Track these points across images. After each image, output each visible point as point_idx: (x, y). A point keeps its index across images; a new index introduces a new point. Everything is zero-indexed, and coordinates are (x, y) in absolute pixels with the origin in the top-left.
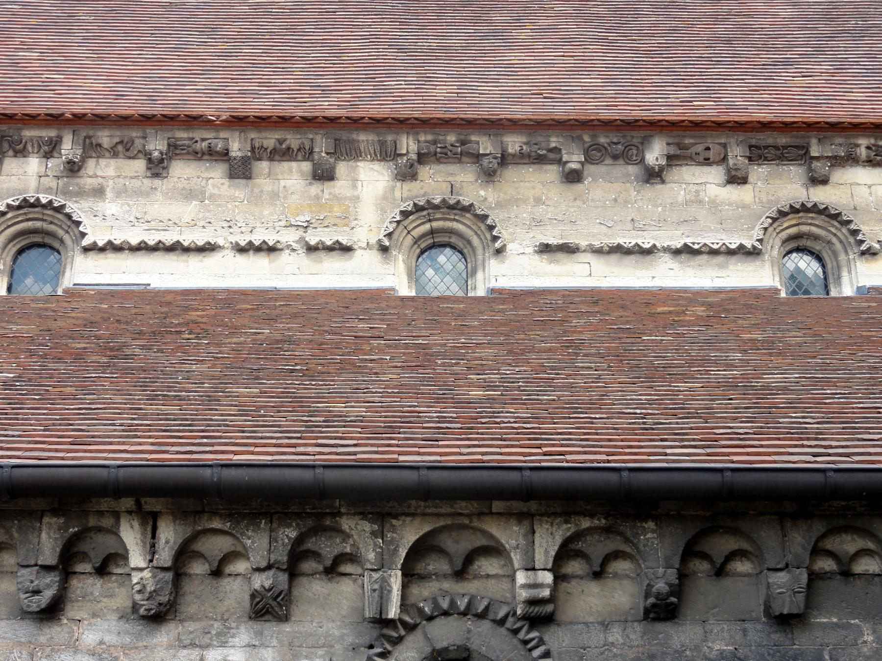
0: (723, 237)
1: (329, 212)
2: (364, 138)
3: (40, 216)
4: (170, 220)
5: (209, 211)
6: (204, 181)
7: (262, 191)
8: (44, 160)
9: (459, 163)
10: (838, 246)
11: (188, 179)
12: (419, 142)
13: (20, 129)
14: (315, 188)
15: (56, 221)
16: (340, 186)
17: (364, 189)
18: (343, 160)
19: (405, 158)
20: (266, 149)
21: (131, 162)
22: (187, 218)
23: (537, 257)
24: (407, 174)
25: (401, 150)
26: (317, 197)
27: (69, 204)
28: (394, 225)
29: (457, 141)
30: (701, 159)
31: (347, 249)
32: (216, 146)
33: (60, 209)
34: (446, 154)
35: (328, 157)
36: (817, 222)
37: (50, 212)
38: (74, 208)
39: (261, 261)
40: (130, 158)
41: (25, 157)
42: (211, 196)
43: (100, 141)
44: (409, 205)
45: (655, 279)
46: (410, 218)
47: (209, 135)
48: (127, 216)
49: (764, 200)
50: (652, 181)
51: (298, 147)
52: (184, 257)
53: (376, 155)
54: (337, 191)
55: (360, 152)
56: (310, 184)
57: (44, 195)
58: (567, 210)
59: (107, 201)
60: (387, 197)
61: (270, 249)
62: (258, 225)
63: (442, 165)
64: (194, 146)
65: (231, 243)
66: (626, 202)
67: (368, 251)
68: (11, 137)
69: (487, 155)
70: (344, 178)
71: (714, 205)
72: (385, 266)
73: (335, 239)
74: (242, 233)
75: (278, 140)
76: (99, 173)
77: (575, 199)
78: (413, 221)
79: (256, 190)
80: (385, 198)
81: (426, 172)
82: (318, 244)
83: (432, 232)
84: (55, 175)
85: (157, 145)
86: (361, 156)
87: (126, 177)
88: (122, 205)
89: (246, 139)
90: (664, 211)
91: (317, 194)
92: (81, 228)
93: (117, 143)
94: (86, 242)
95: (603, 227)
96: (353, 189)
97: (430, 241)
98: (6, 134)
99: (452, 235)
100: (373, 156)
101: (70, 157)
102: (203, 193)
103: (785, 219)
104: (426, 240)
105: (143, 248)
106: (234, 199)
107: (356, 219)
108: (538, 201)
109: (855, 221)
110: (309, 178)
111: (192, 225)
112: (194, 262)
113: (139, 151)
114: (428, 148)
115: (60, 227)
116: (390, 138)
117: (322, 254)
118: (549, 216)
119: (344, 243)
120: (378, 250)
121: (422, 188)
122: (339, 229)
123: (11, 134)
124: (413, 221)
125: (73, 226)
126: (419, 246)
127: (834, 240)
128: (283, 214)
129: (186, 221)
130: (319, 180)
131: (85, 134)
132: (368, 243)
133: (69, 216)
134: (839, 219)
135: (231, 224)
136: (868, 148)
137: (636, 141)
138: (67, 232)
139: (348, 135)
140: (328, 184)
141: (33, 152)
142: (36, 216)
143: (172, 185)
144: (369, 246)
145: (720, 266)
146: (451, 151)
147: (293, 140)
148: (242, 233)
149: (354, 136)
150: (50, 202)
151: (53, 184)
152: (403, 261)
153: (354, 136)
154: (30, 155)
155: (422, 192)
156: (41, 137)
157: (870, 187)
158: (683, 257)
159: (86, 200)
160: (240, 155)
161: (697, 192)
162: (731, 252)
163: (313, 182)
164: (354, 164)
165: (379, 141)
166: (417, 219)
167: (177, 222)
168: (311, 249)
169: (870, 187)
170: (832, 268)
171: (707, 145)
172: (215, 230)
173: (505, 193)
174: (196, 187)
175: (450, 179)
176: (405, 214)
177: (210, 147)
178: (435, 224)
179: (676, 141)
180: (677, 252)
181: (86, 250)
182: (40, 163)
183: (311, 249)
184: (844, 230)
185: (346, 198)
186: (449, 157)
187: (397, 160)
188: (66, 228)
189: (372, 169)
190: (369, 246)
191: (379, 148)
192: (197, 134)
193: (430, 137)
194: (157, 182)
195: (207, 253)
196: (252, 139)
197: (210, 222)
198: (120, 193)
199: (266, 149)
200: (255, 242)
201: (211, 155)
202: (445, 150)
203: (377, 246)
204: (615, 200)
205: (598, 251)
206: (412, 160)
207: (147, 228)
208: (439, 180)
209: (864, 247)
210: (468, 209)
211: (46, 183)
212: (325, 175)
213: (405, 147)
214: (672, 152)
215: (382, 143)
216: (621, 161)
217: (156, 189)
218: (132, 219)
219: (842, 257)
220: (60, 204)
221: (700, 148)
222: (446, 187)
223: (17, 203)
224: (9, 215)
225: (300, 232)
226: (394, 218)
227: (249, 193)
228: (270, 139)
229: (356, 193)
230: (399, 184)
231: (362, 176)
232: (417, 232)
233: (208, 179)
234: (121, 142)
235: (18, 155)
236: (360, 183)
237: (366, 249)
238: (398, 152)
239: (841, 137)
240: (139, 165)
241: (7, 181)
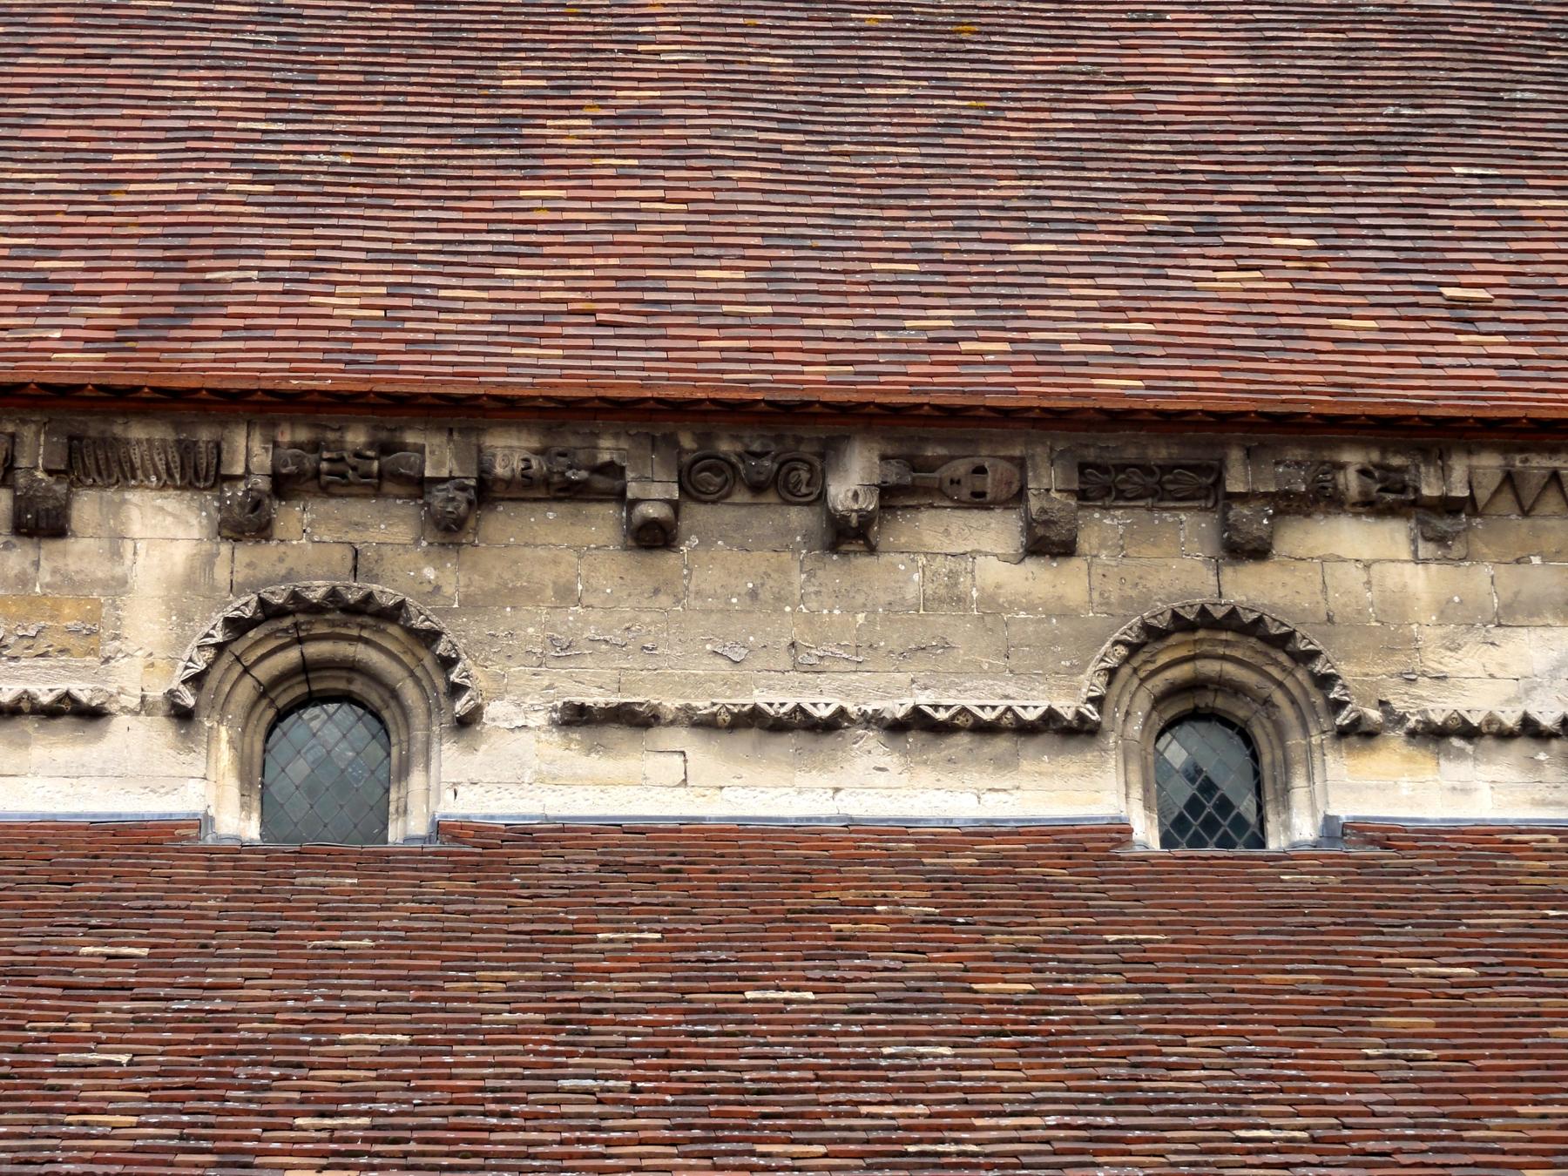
0: (1011, 690)
1: (52, 618)
9: (376, 496)
10: (1288, 713)
12: (276, 445)
17: (141, 559)
18: (91, 487)
19: (241, 486)
23: (556, 737)
25: (231, 465)
26: (23, 581)
28: (209, 654)
29: (370, 445)
30: (965, 493)
31: (90, 715)
34: (343, 475)
35: (52, 480)
36: (1238, 654)
44: (246, 604)
45: (840, 795)
46: (251, 634)
49: (1113, 599)
50: (845, 548)
53: (171, 476)
54: (72, 564)
55: (133, 469)
58: (635, 619)
60: (195, 581)
63: (333, 502)
66: (780, 599)
67: (142, 718)
69: (443, 480)
70: (90, 531)
71: (992, 607)
72: (182, 758)
73: (62, 687)
77: (656, 591)
78: (257, 643)
80: (189, 583)
81: (292, 518)
82: (19, 699)
83: (305, 668)
86: (134, 477)
90: (870, 622)
91: (24, 572)
95: (720, 662)
96: (111, 559)
97: (300, 690)
99: (355, 676)
100: (165, 477)
103: (1159, 646)
104: (291, 687)
107: (116, 637)
108: (566, 595)
109: (1327, 654)
114: (298, 460)
116: (205, 435)
117: (30, 725)
118: (591, 633)
119: (85, 700)
120: (168, 716)
121: (281, 560)
122: (75, 662)
124: (257, 643)
126: (272, 701)
127: (1278, 697)
132: (143, 698)
134: (1290, 647)
136: (1363, 472)
137: (806, 450)
139: (102, 427)
140: (50, 546)
144: (145, 706)
145: (1003, 764)
146: (354, 469)
149: (118, 430)
152: (231, 741)
153: (118, 430)
155: (282, 569)
157: (1367, 567)
158: (912, 738)
161: (952, 574)
162: (1025, 730)
163: (14, 540)
164: (117, 498)
165: (179, 442)
166: (267, 637)
169: (1367, 567)
170: (1273, 763)
171: (977, 461)
173: (486, 575)
175: (352, 536)
176: (237, 626)
178: (314, 650)
179: (905, 450)
180: (896, 728)
184: (1301, 675)
185: (95, 583)
186: (350, 484)
187: (222, 491)
189: (161, 509)
190: (145, 706)
191: (177, 459)
193: (303, 435)
202: (340, 467)
203: (166, 707)
204: (753, 594)
205: (707, 724)
206: (259, 491)
208: (326, 538)
209: (1343, 719)
210: (395, 613)
212: (43, 524)
213: (242, 458)
214: (892, 479)
215: (186, 449)
216: (771, 498)
219: (1295, 740)
221: (961, 468)
222: (340, 558)
226: (208, 635)
229: (118, 571)
230: (225, 549)
231: (136, 528)
232: (264, 671)
236: (129, 545)
237: (138, 714)
238: (224, 471)
239: (1300, 445)
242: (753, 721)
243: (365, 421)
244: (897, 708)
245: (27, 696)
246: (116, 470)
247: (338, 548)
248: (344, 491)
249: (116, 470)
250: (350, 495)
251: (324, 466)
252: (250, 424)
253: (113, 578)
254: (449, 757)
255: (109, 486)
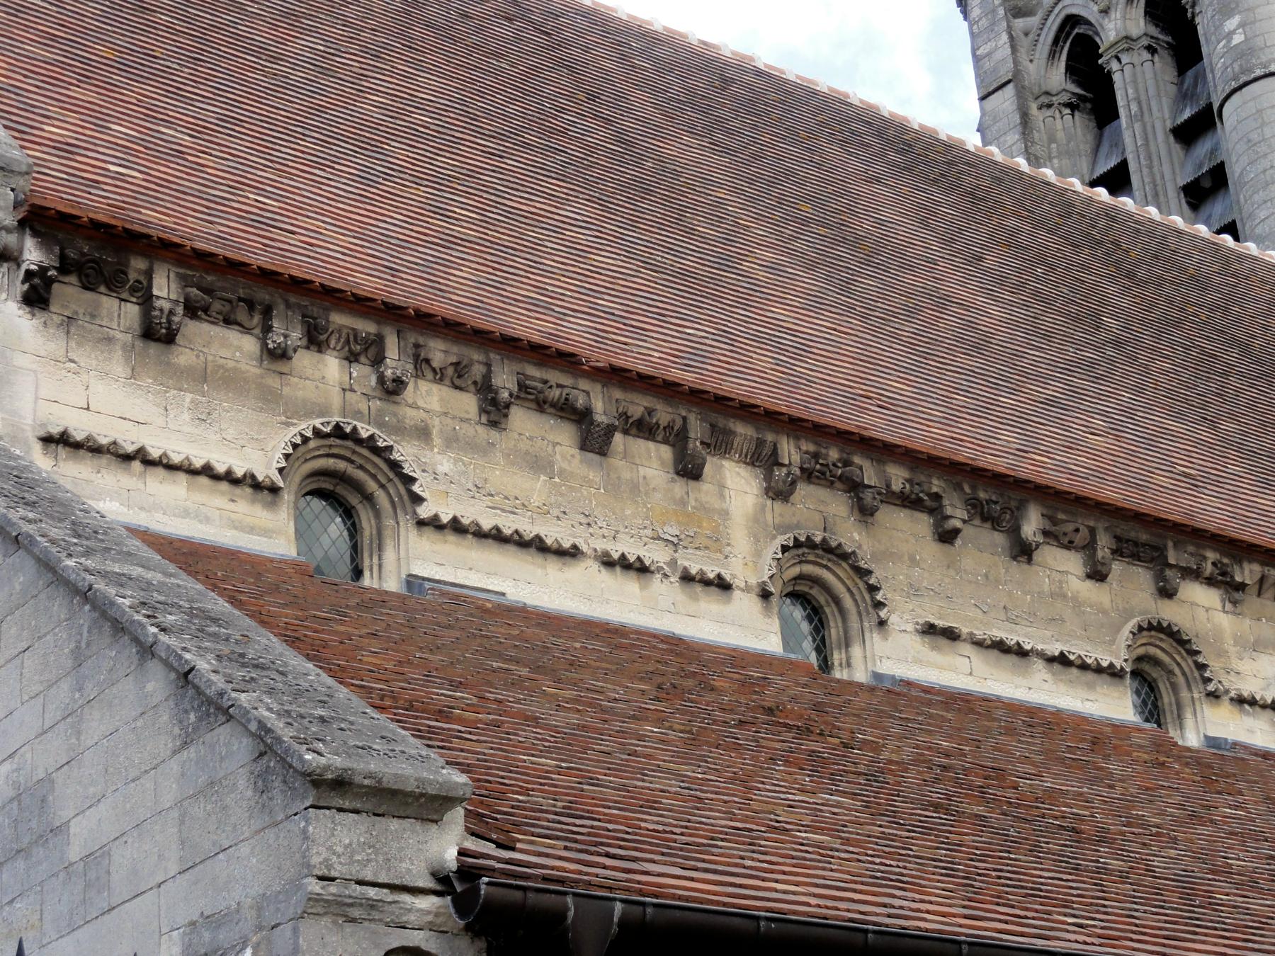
0: (1089, 649)
2: (743, 431)
3: (348, 454)
4: (517, 498)
5: (562, 495)
6: (550, 448)
7: (619, 478)
8: (346, 363)
9: (829, 487)
10: (1181, 680)
11: (531, 438)
13: (327, 310)
14: (680, 487)
15: (369, 467)
16: (705, 489)
19: (784, 470)
20: (628, 417)
21: (457, 393)
22: (536, 501)
23: (918, 638)
24: (779, 493)
25: (783, 457)
27: (396, 447)
29: (839, 460)
30: (1065, 541)
31: (723, 585)
32: (577, 401)
33: (370, 444)
34: (823, 474)
36: (1163, 645)
37: (365, 452)
38: (405, 453)
39: (629, 585)
40: (457, 387)
41: (320, 351)
42: (561, 473)
43: (430, 356)
45: (1032, 691)
47: (566, 380)
48: (463, 481)
49: (1120, 607)
50: (1019, 559)
51: (666, 424)
52: (539, 559)
53: (746, 456)
54: (704, 498)
55: (731, 448)
56: (673, 480)
57: (363, 425)
58: (942, 580)
59: (436, 450)
60: (757, 518)
61: (641, 569)
62: (622, 529)
64: (547, 393)
65: (595, 550)
66: (998, 581)
68: (315, 319)
69: (870, 487)
71: (1077, 603)
73: (717, 570)
74: (604, 537)
75: (646, 408)
76: (421, 403)
77: (948, 567)
79: (613, 476)
84: (364, 391)
85: (505, 380)
87: (454, 418)
88: (456, 461)
89: (610, 397)
90: (1033, 601)
91: (682, 497)
92: (416, 488)
93: (452, 364)
94: (424, 512)
95: (978, 610)
98: (310, 313)
99: (816, 585)
101: (398, 373)
102: (551, 464)
105: (497, 536)
106: (590, 484)
107: (729, 545)
108: (913, 562)
109: (1204, 653)
110: (672, 471)
111: (543, 511)
112: (552, 570)
113: (475, 383)
115: (374, 477)
116: (770, 437)
117: (698, 588)
118: (925, 584)
120: (758, 595)
123: (315, 315)
125: (396, 480)
127: (1177, 671)
128: (647, 518)
129: (536, 504)
130: (683, 476)
131: (412, 340)
133: (395, 466)
134: (1188, 646)
135: (590, 519)
136: (1214, 564)
137: (1013, 504)
138: (382, 486)
139: (725, 422)
140: (692, 483)
141: (334, 349)
142: (342, 452)
143: (513, 442)
144: (747, 589)
145: (1091, 686)
146: (830, 471)
147: (664, 414)
148: (604, 537)
150: (372, 437)
151: (363, 406)
154: (329, 351)
156: (354, 329)
157: (1207, 611)
158: (1056, 666)
159: (408, 442)
160: (606, 422)
161: (1060, 582)
163: (676, 477)
164: (718, 462)
165: (758, 439)
167: (526, 503)
168: (687, 578)
169: (1207, 611)
170: (1170, 704)
171: (1077, 525)
172: (573, 526)
173: (879, 542)
174: (542, 455)
175: (821, 508)
177: (566, 399)
179: (1050, 513)
180: (1051, 660)
181: (421, 523)
182: (342, 366)
183: (687, 578)
184: (1190, 661)
186: (826, 479)
188: (383, 481)
192: (555, 376)
194: (494, 435)
195: (568, 559)
196: (617, 400)
197: (564, 513)
198: (452, 441)
199: (628, 417)
200: (629, 556)
201: (562, 409)
202: (825, 469)
203: (757, 590)
204: (986, 576)
205: (979, 644)
207: (490, 504)
209: (1211, 687)
210: (845, 556)
211: (353, 402)
214: (1047, 528)
215: (760, 443)
216: (988, 525)
217: (492, 444)
218: (470, 486)
220: (385, 444)
221: (1070, 527)
223: (328, 429)
224: (312, 444)
225: (670, 549)
227: (605, 478)
228: (638, 405)
230: (769, 502)
231: (729, 483)
233: (556, 444)
234: (456, 364)
235: (312, 348)
239: (1193, 544)
240: (468, 403)
241: (300, 386)
242: (1000, 647)
243: (837, 446)
244: (1054, 649)
245: (702, 572)
246: (724, 447)
247: (817, 513)
248: (817, 481)
249: (723, 450)
250: (819, 484)
251: (818, 467)
252: (788, 436)
253: (723, 510)
254: (875, 640)
255: (714, 455)
